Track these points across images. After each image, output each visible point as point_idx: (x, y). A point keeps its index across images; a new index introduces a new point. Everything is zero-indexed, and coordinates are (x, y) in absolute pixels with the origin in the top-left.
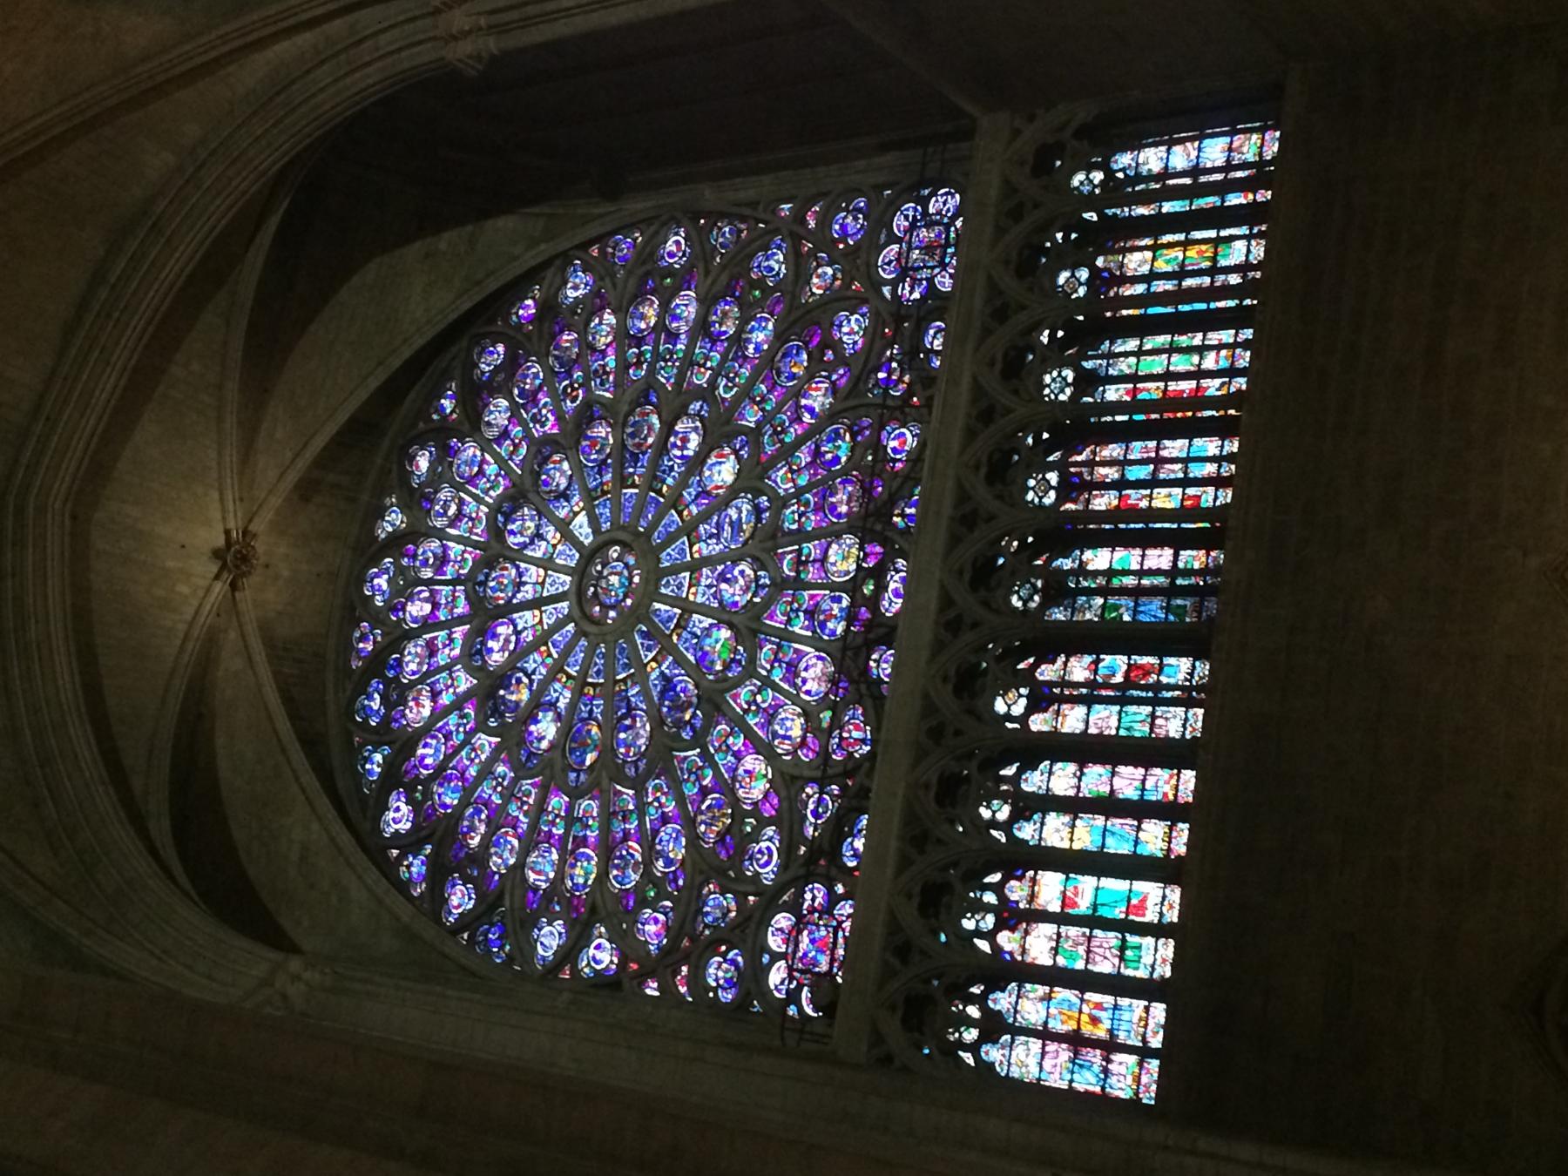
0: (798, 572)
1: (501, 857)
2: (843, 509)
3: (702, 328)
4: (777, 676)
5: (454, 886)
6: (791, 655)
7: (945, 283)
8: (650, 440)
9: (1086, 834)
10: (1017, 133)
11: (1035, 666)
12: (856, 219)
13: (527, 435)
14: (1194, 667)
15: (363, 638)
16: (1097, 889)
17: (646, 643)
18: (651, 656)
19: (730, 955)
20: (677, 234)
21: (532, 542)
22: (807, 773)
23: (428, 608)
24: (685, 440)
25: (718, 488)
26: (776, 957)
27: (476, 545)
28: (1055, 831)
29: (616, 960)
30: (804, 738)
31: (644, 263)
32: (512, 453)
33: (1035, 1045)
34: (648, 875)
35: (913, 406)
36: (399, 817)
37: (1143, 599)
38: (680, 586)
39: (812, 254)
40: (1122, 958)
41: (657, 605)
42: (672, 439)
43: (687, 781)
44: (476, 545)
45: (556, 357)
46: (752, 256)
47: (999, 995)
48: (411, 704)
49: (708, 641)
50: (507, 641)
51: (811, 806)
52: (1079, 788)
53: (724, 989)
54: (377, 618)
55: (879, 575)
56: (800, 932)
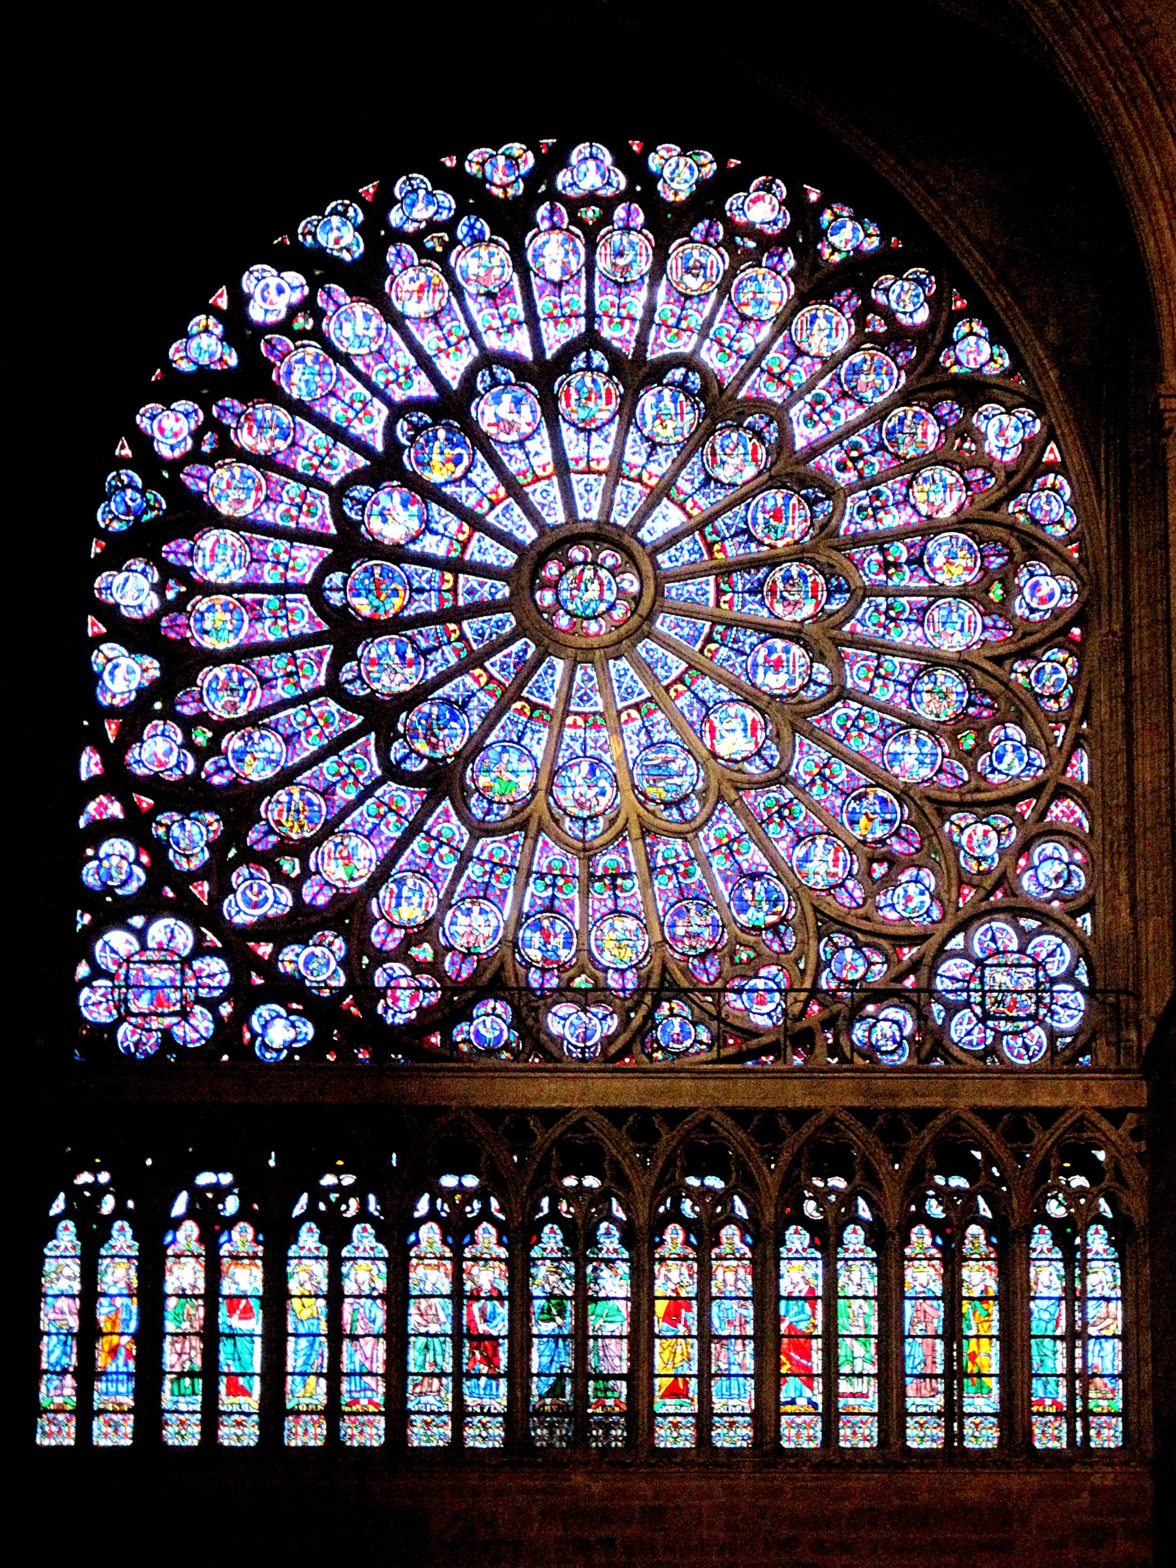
0: (601, 879)
1: (229, 485)
2: (680, 931)
3: (931, 662)
4: (474, 871)
5: (187, 415)
8: (779, 609)
9: (305, 1313)
12: (1057, 878)
14: (495, 1415)
16: (251, 1335)
17: (511, 661)
18: (494, 671)
19: (138, 871)
20: (1064, 591)
23: (554, 273)
24: (777, 665)
25: (713, 730)
26: (141, 934)
27: (642, 341)
28: (307, 1273)
29: (116, 702)
31: (1026, 546)
32: (772, 375)
33: (77, 1287)
34: (221, 728)
36: (271, 292)
40: (181, 1375)
41: (560, 665)
42: (779, 644)
43: (340, 764)
44: (642, 341)
45: (901, 421)
46: (1020, 723)
47: (129, 1232)
48: (423, 279)
49: (514, 755)
50: (511, 427)
51: (318, 951)
52: (359, 1297)
53: (100, 866)
55: (597, 995)
56: (173, 963)
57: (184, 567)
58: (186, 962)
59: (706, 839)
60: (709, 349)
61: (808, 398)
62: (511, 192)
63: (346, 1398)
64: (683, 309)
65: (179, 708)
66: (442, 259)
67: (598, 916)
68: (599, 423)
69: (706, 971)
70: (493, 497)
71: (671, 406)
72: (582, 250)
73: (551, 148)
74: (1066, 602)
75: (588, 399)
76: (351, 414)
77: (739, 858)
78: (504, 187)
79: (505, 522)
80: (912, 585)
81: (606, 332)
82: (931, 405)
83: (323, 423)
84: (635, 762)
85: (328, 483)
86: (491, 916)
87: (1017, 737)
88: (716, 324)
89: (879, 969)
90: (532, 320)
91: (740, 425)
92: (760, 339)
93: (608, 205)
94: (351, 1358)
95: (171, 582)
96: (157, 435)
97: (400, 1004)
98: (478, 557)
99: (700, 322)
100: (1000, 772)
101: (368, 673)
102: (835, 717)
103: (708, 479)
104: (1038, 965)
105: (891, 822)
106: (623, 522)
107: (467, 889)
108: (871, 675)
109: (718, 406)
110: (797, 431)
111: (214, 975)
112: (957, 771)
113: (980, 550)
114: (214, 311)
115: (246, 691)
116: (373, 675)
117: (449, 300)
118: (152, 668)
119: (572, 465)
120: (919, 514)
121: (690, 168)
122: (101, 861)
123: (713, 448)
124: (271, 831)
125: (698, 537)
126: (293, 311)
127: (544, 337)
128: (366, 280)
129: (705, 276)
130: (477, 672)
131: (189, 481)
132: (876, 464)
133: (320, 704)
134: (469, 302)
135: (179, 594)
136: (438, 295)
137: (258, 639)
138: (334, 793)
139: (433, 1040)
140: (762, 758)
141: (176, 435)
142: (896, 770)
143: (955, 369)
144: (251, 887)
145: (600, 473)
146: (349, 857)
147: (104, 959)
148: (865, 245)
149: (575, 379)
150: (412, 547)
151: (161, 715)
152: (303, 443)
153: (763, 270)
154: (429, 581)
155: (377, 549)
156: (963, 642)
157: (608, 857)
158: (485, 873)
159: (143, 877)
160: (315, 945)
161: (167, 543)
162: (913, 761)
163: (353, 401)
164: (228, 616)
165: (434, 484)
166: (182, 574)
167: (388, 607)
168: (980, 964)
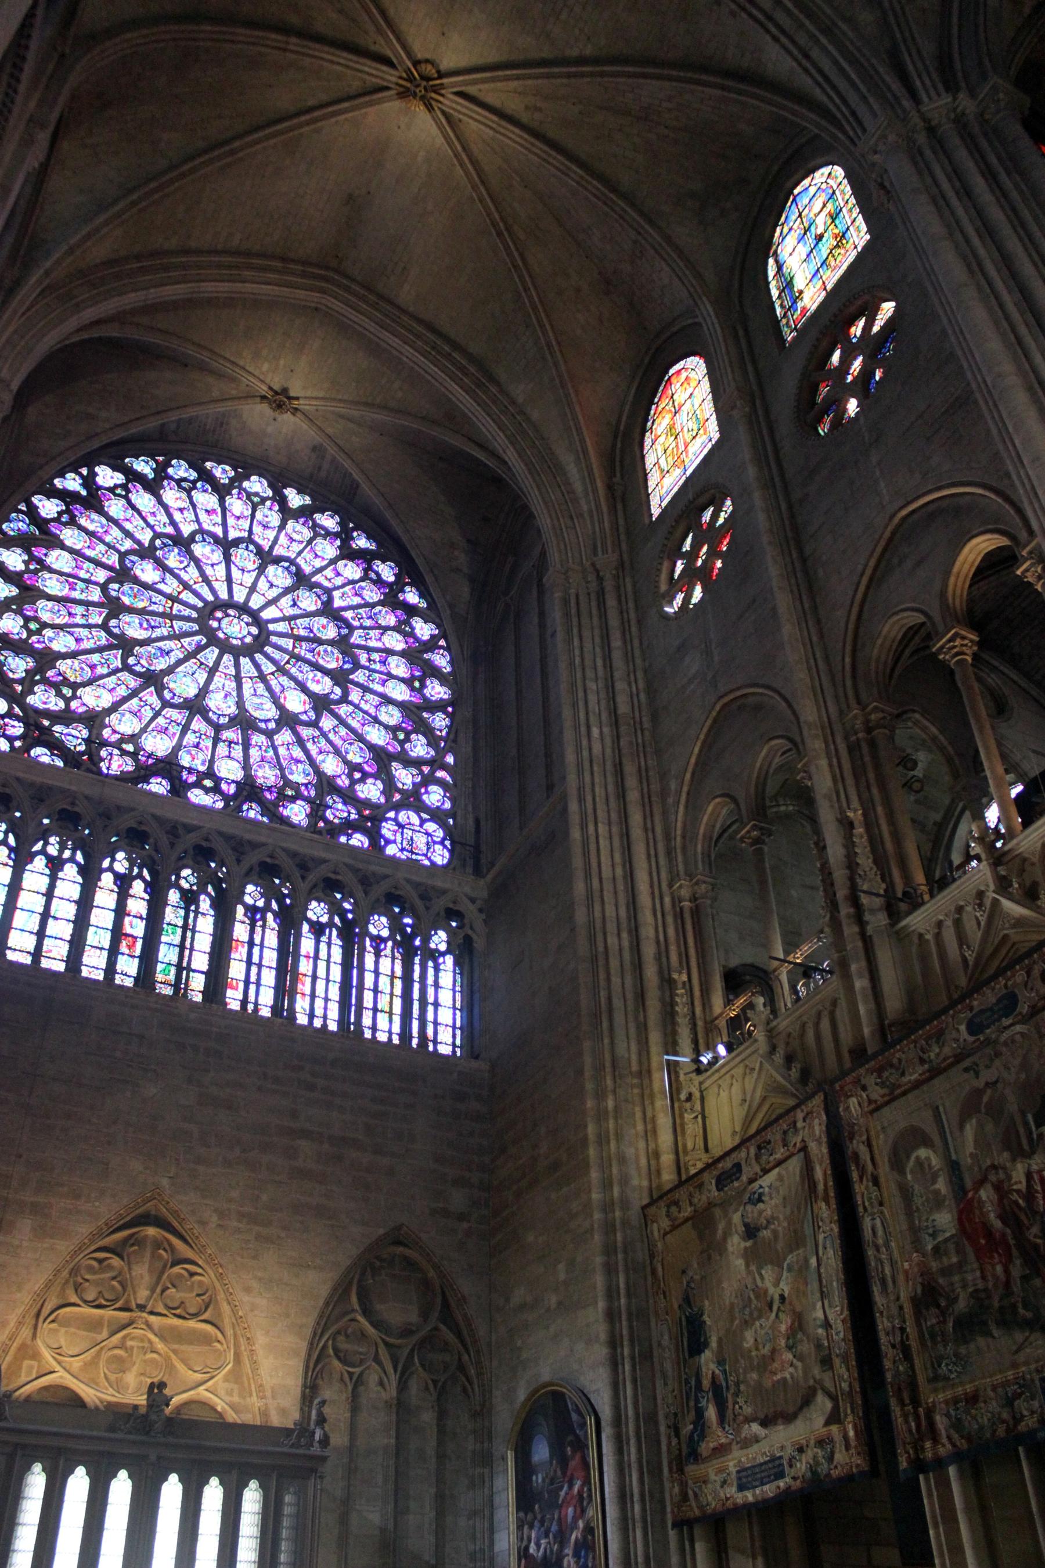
3: (387, 700)
4: (160, 720)
7: (391, 850)
10: (473, 901)
11: (144, 880)
15: (224, 471)
22: (95, 732)
24: (318, 682)
27: (272, 548)
34: (44, 625)
36: (107, 476)
37: (177, 950)
39: (421, 772)
41: (217, 651)
42: (319, 674)
44: (272, 548)
63: (45, 948)
66: (189, 492)
74: (446, 697)
81: (256, 539)
93: (263, 500)
94: (52, 928)
103: (295, 604)
109: (301, 580)
118: (15, 591)
124: (60, 674)
126: (116, 486)
149: (240, 551)
151: (13, 611)
155: (136, 580)
162: (377, 736)
166: (40, 562)
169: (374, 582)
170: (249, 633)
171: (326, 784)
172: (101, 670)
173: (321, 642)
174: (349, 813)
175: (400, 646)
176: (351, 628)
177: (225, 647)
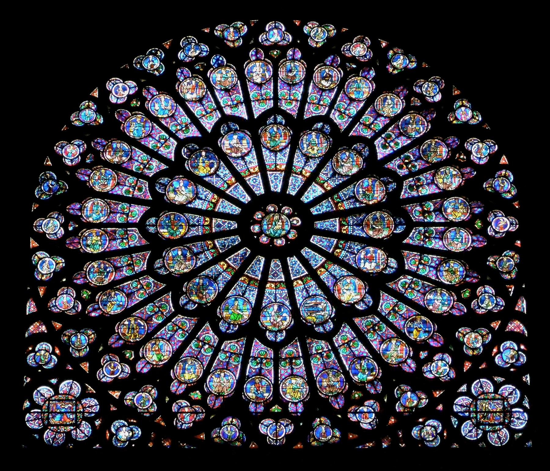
0: (285, 359)
1: (99, 179)
2: (325, 384)
4: (221, 356)
5: (79, 146)
6: (233, 363)
8: (371, 233)
12: (512, 358)
13: (377, 135)
20: (512, 224)
21: (304, 155)
23: (259, 81)
24: (371, 259)
25: (339, 290)
26: (56, 388)
27: (301, 110)
29: (43, 278)
30: (185, 383)
32: (365, 125)
34: (95, 290)
35: (389, 419)
36: (120, 90)
38: (275, 275)
39: (492, 330)
41: (263, 260)
42: (372, 249)
44: (301, 110)
45: (429, 146)
48: (194, 82)
49: (240, 302)
50: (237, 150)
51: (143, 395)
53: (34, 356)
54: (251, 39)
55: (285, 414)
57: (77, 215)
58: (79, 399)
59: (337, 340)
60: (334, 114)
61: (383, 136)
62: (236, 44)
64: (321, 95)
65: (75, 281)
67: (283, 377)
68: (281, 148)
69: (338, 403)
70: (229, 182)
71: (316, 140)
72: (271, 70)
73: (255, 24)
74: (513, 229)
75: (276, 137)
76: (159, 145)
77: (354, 350)
78: (233, 42)
79: (235, 193)
80: (436, 221)
81: (284, 106)
82: (444, 138)
83: (145, 149)
84: (300, 305)
85: (148, 176)
86: (229, 378)
87: (490, 292)
88: (338, 103)
89: (424, 402)
90: (247, 101)
91: (350, 148)
92: (359, 109)
95: (71, 223)
96: (64, 155)
97: (185, 420)
98: (221, 210)
99: (330, 101)
100: (482, 308)
101: (168, 264)
102: (400, 283)
104: (504, 399)
105: (429, 332)
106: (293, 193)
107: (218, 365)
108: (417, 263)
109: (340, 140)
110: (378, 151)
111: (92, 406)
112: (462, 308)
113: (470, 205)
114: (93, 99)
115: (108, 273)
116: (172, 265)
117: (206, 92)
119: (268, 167)
120: (440, 189)
121: (324, 32)
122: (36, 352)
123: (337, 159)
124: (120, 338)
125: (330, 200)
127: (254, 109)
128: (167, 84)
129: (332, 81)
130: (222, 263)
131: (80, 177)
132: (419, 165)
133: (145, 279)
134: (217, 94)
135: (74, 228)
136: (201, 91)
137: (114, 248)
138: (151, 320)
139: (202, 436)
140: (364, 302)
141: (73, 155)
142: (431, 307)
143: (455, 122)
144: (110, 365)
145: (282, 171)
146: (158, 350)
147: (38, 399)
148: (410, 66)
149: (269, 128)
150: (189, 206)
151: (64, 284)
152: (136, 158)
153: (360, 78)
154: (198, 221)
156: (462, 248)
157: (288, 349)
158: (227, 357)
159: (56, 360)
160: (142, 392)
161: (69, 204)
162: (440, 303)
163: (160, 139)
164: (99, 238)
165: (201, 177)
166: (77, 219)
167: (178, 233)
168: (475, 398)
169: (418, 110)
170: (293, 227)
171: (392, 375)
172: (157, 321)
173: (368, 209)
174: (420, 399)
175: (455, 183)
176: (399, 180)
177: (270, 252)
